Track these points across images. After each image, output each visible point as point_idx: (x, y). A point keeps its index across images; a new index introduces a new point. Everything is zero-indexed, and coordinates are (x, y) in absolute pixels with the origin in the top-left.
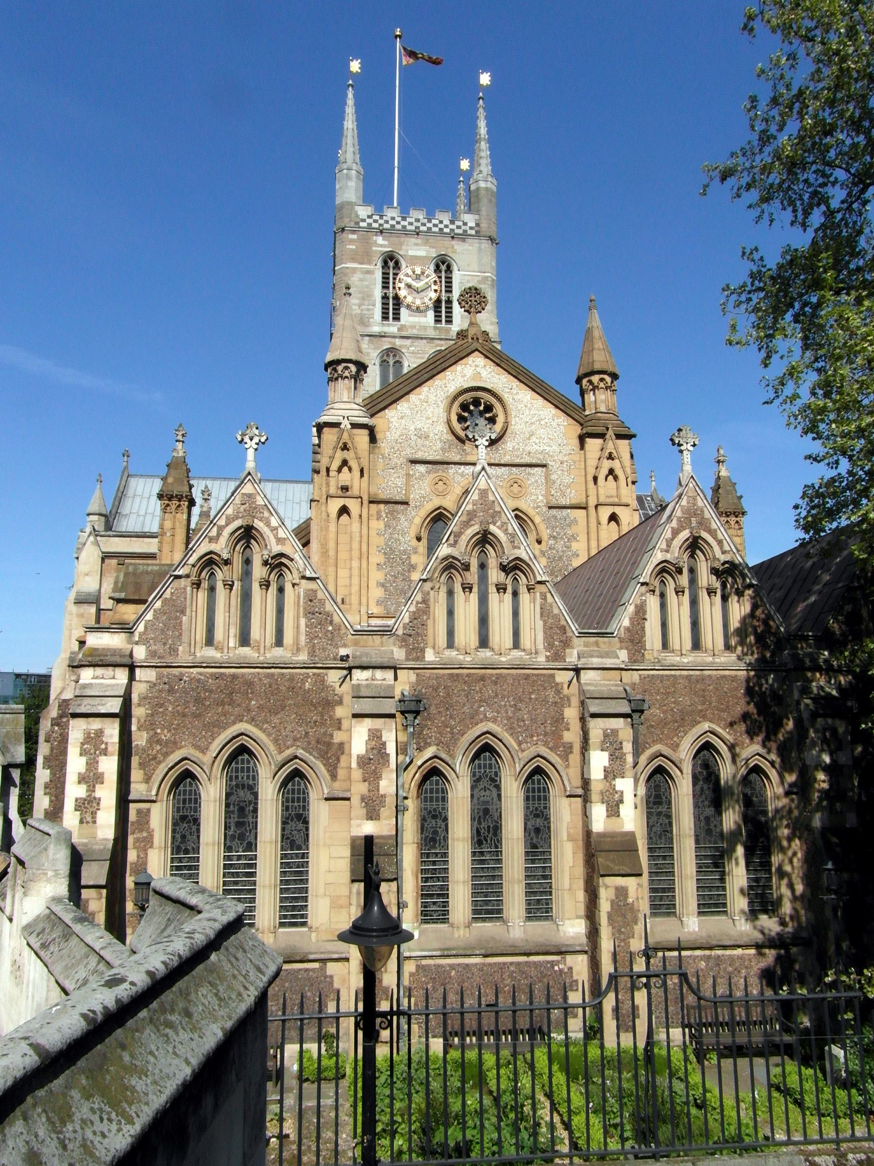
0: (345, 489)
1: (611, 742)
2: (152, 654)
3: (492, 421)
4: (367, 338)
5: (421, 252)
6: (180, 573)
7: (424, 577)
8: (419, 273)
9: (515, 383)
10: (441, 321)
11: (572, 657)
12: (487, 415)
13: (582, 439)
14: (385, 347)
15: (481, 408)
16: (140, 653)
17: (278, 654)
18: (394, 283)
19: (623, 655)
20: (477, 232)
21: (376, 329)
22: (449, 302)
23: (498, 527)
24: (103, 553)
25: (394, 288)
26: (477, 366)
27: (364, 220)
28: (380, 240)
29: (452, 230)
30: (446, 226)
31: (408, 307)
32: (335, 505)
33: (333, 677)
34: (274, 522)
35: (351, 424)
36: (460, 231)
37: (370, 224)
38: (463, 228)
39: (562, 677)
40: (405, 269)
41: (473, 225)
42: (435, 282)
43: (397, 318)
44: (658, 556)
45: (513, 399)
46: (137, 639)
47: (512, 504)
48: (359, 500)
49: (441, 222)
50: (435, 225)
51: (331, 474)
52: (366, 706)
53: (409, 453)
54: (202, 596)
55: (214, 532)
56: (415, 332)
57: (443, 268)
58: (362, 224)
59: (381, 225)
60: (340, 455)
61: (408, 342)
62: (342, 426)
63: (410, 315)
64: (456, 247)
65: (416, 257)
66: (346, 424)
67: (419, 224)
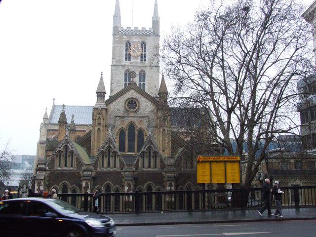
0: (99, 124)
1: (129, 185)
2: (49, 168)
4: (121, 67)
5: (137, 40)
9: (141, 96)
11: (125, 169)
16: (47, 168)
17: (71, 168)
19: (134, 169)
21: (124, 64)
22: (145, 55)
28: (125, 37)
31: (133, 57)
32: (97, 128)
33: (81, 173)
34: (71, 144)
39: (122, 173)
43: (130, 60)
44: (142, 150)
47: (139, 126)
52: (86, 178)
53: (115, 114)
54: (58, 158)
60: (98, 116)
61: (131, 67)
66: (99, 108)
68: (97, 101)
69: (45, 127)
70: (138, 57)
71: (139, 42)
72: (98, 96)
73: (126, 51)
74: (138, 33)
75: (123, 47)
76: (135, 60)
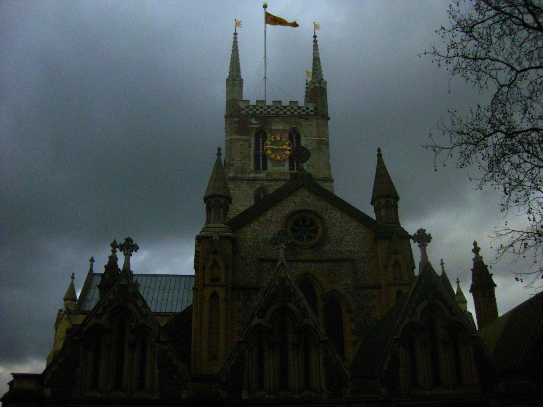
3: (315, 231)
5: (280, 127)
6: (77, 338)
7: (241, 340)
8: (279, 139)
10: (294, 169)
12: (312, 228)
13: (375, 240)
14: (257, 187)
15: (308, 223)
18: (263, 147)
20: (316, 114)
21: (252, 175)
23: (293, 304)
24: (72, 325)
25: (263, 150)
26: (304, 196)
27: (243, 110)
28: (254, 121)
29: (299, 113)
30: (296, 111)
31: (272, 160)
32: (208, 292)
35: (219, 237)
36: (305, 113)
37: (247, 112)
38: (306, 111)
40: (270, 138)
41: (312, 109)
42: (289, 144)
43: (265, 168)
45: (329, 216)
46: (46, 383)
48: (225, 287)
49: (292, 108)
50: (289, 110)
51: (207, 270)
55: (100, 311)
56: (277, 176)
57: (294, 136)
58: (242, 112)
59: (254, 112)
61: (273, 183)
62: (214, 238)
63: (274, 166)
64: (302, 122)
65: (277, 130)
67: (278, 110)
68: (208, 221)
69: (69, 319)
70: (285, 160)
71: (284, 130)
72: (208, 209)
73: (257, 148)
74: (282, 113)
75: (249, 140)
76: (278, 168)
